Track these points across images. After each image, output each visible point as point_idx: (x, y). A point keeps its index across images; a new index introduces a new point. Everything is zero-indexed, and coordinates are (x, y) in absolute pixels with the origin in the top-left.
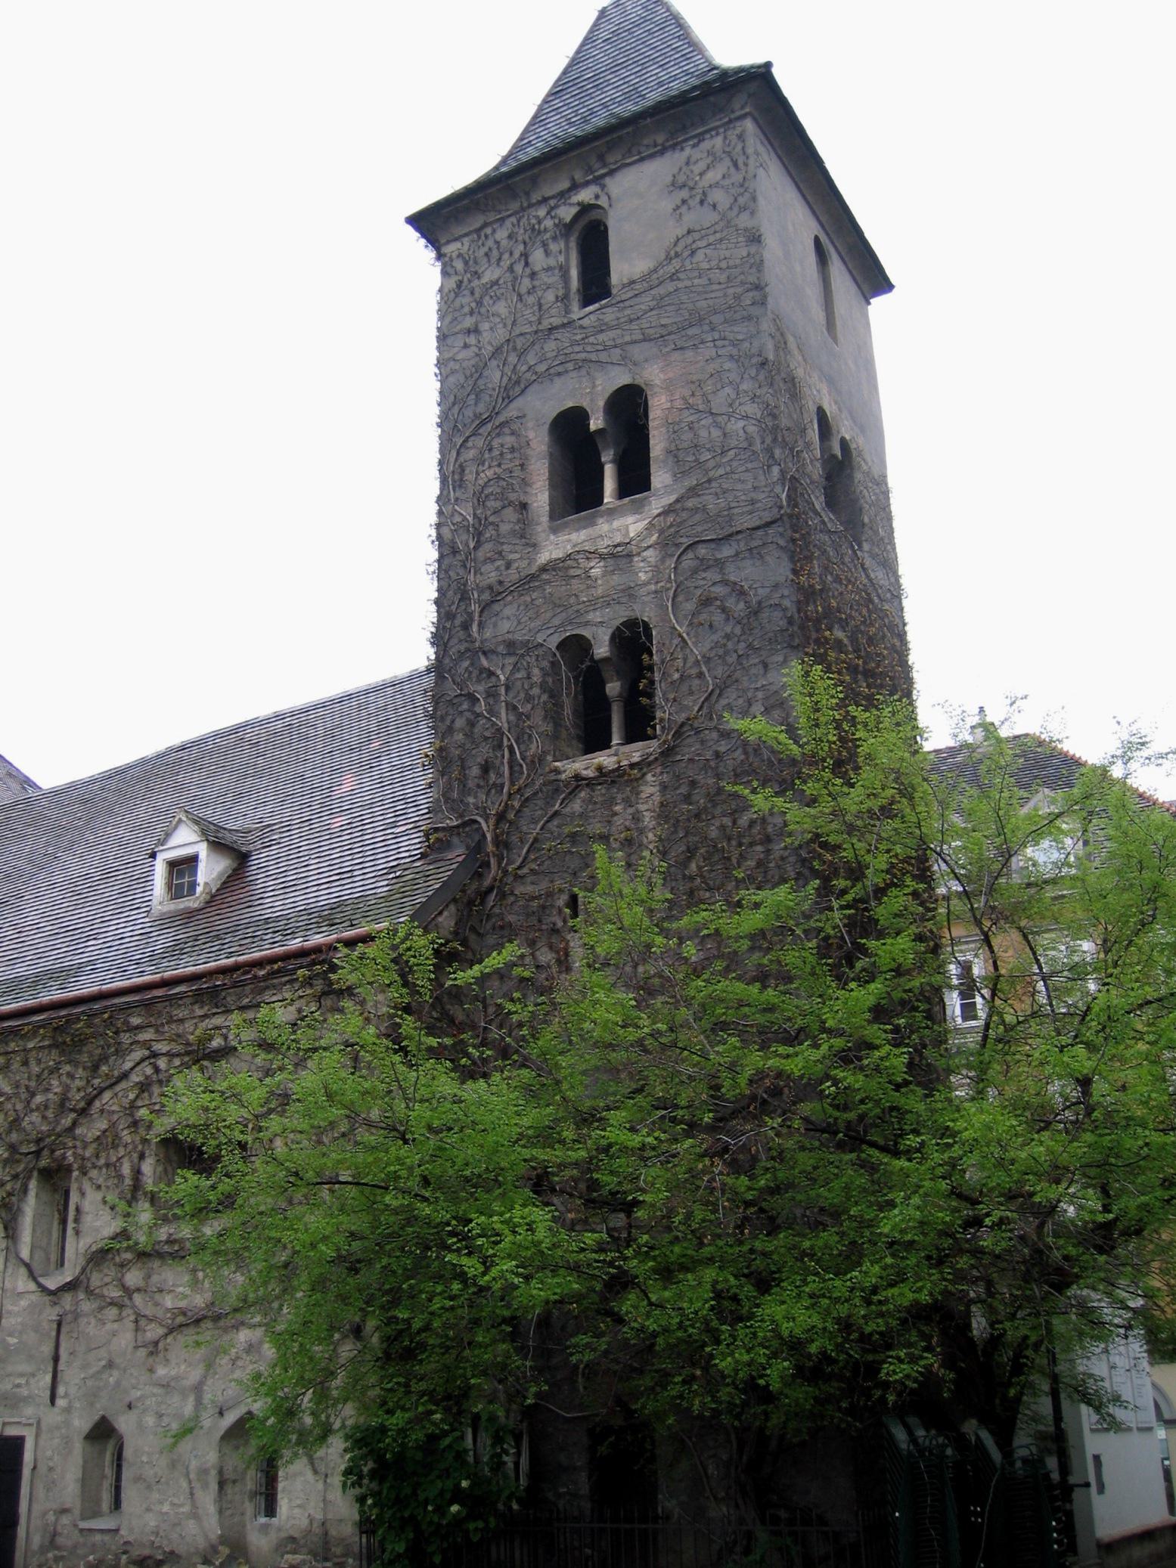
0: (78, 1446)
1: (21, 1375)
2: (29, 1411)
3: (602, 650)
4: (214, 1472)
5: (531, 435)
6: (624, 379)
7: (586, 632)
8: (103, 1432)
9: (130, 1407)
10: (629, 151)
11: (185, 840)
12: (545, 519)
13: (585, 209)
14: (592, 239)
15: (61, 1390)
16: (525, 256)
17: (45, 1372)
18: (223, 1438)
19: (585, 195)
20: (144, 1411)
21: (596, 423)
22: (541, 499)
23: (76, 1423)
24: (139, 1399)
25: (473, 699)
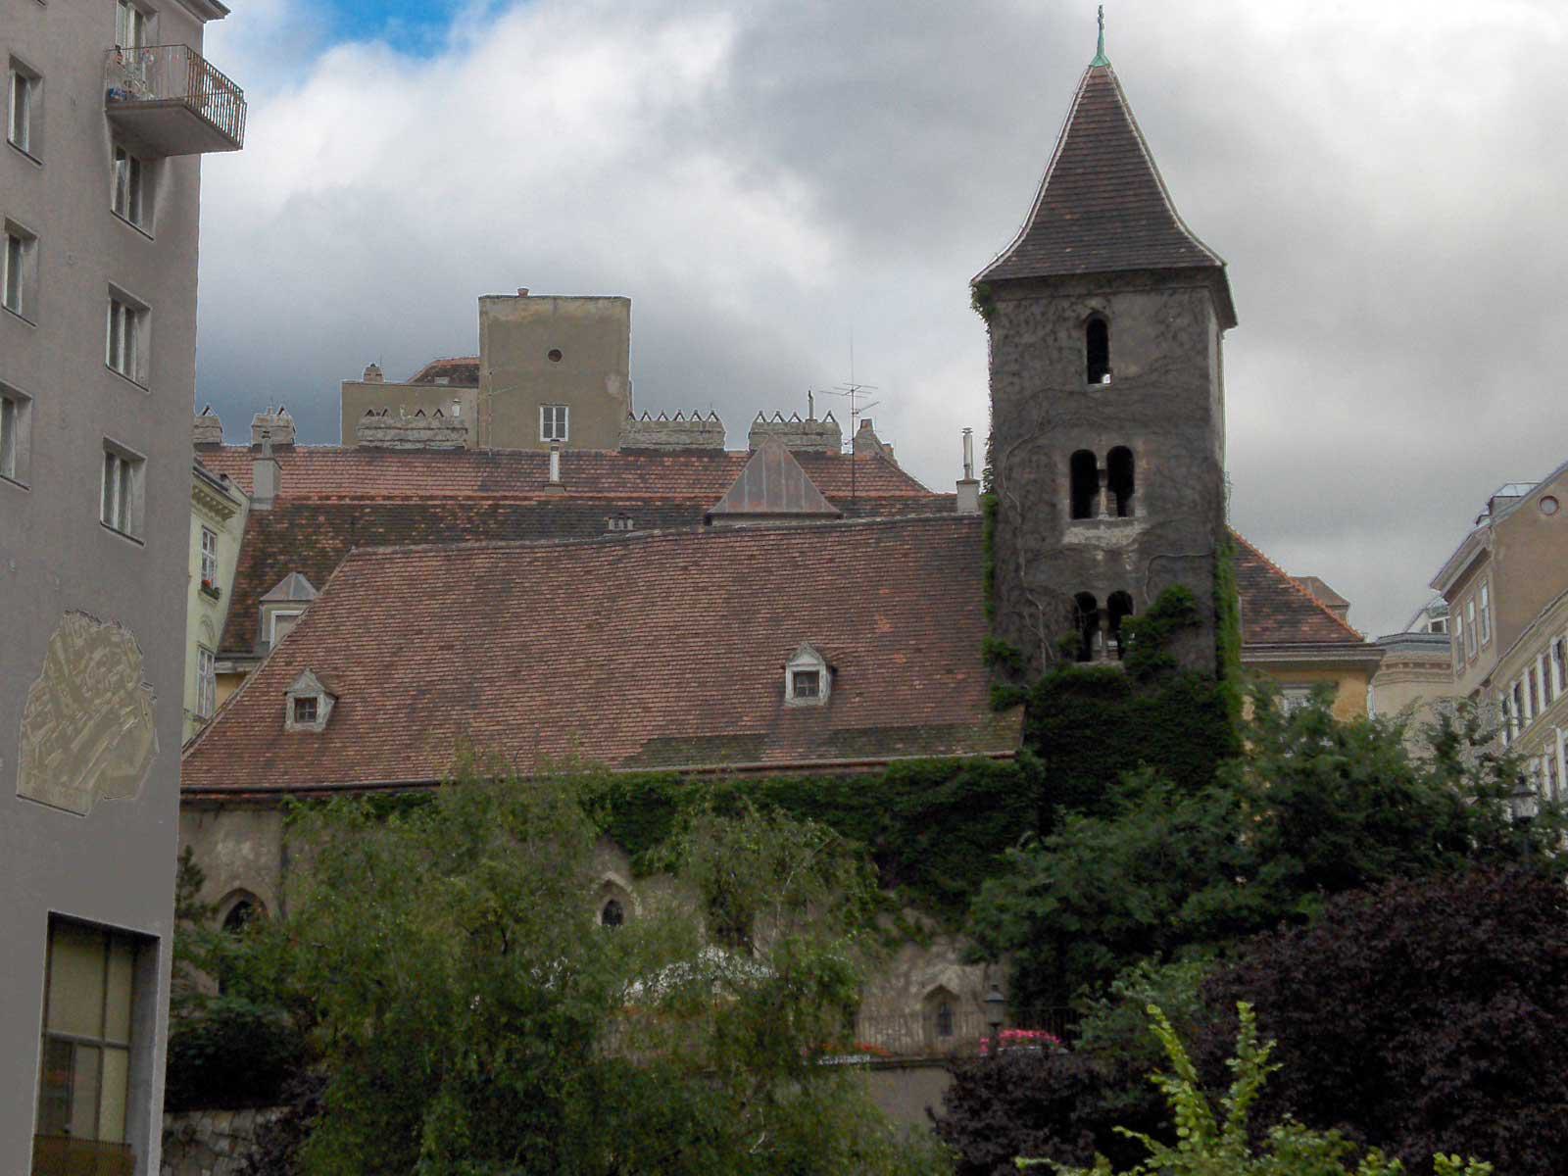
7: (1094, 593)
11: (806, 661)
13: (1095, 312)
14: (1097, 332)
16: (1054, 332)
22: (1065, 503)
25: (1021, 616)
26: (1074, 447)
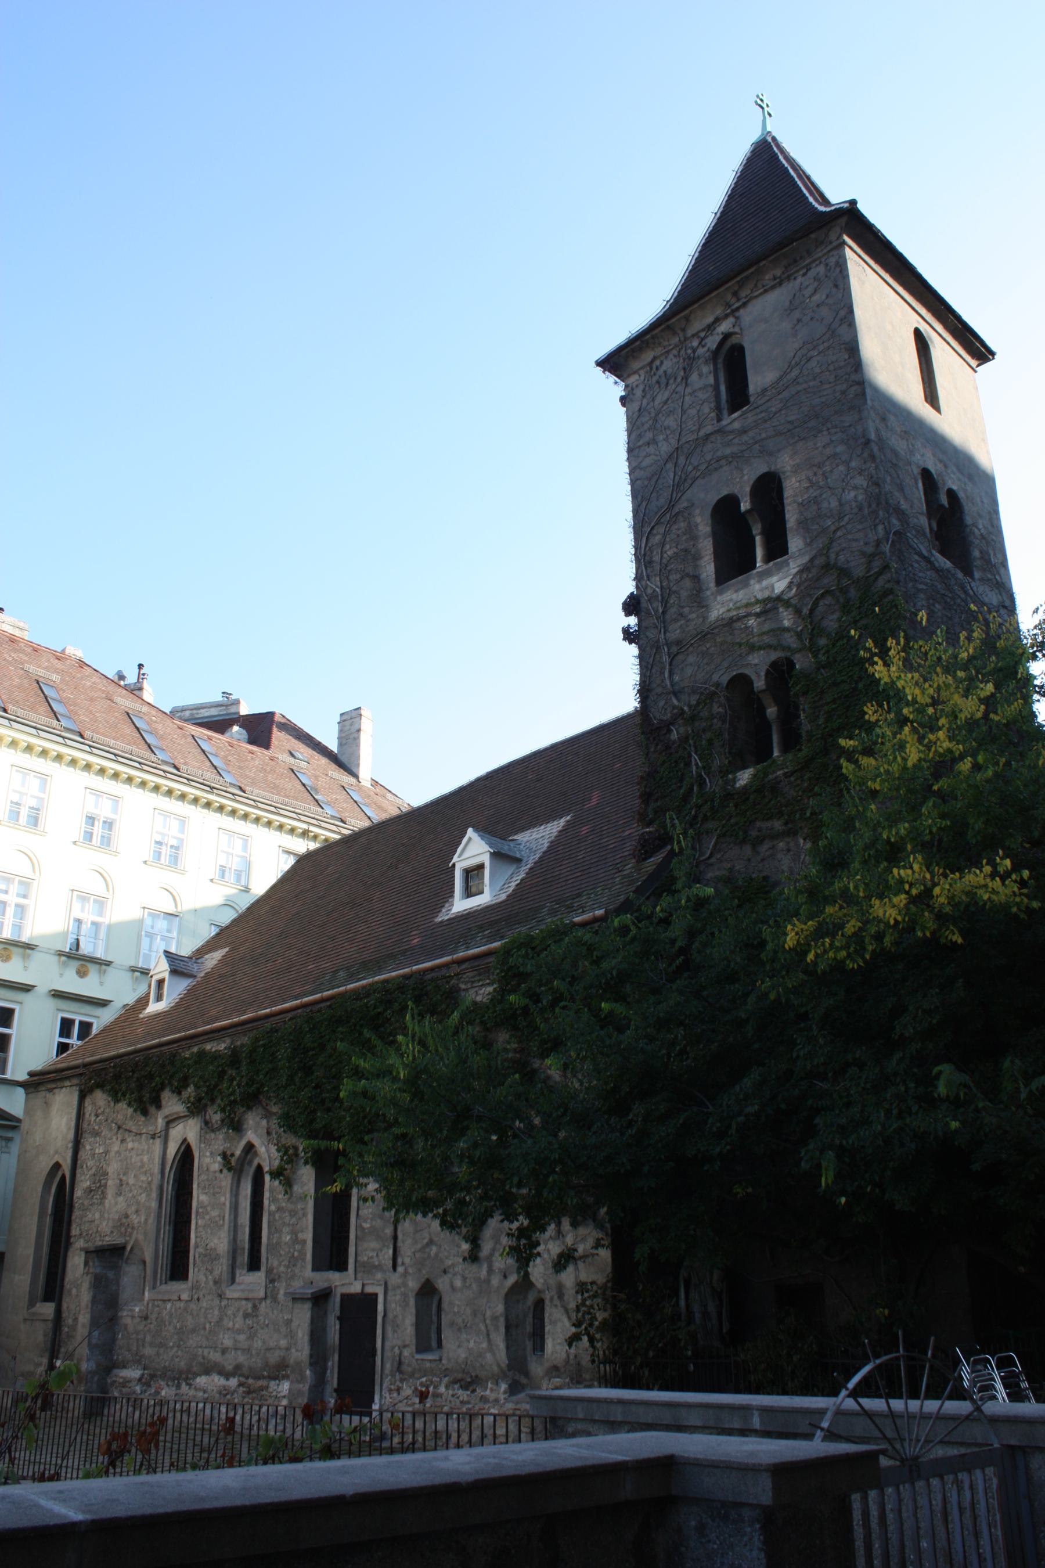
0: (412, 1302)
1: (373, 1250)
2: (379, 1276)
3: (760, 684)
4: (502, 1320)
5: (698, 520)
6: (764, 469)
7: (746, 671)
8: (428, 1292)
9: (445, 1272)
10: (756, 285)
12: (712, 585)
14: (733, 361)
15: (399, 1261)
17: (388, 1248)
18: (507, 1295)
19: (724, 327)
20: (455, 1275)
21: (745, 506)
22: (708, 569)
23: (410, 1284)
24: (449, 1267)
26: (714, 498)
